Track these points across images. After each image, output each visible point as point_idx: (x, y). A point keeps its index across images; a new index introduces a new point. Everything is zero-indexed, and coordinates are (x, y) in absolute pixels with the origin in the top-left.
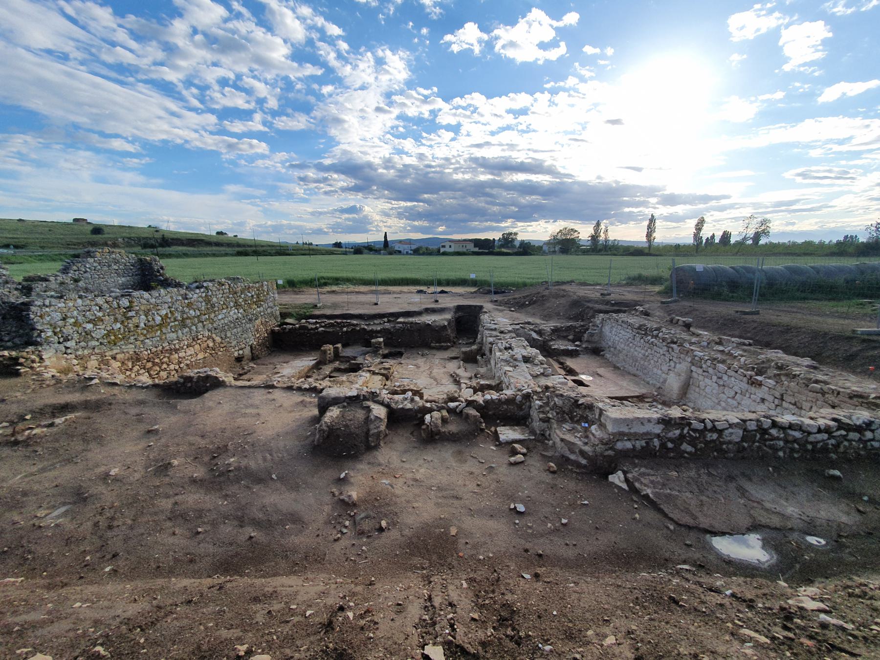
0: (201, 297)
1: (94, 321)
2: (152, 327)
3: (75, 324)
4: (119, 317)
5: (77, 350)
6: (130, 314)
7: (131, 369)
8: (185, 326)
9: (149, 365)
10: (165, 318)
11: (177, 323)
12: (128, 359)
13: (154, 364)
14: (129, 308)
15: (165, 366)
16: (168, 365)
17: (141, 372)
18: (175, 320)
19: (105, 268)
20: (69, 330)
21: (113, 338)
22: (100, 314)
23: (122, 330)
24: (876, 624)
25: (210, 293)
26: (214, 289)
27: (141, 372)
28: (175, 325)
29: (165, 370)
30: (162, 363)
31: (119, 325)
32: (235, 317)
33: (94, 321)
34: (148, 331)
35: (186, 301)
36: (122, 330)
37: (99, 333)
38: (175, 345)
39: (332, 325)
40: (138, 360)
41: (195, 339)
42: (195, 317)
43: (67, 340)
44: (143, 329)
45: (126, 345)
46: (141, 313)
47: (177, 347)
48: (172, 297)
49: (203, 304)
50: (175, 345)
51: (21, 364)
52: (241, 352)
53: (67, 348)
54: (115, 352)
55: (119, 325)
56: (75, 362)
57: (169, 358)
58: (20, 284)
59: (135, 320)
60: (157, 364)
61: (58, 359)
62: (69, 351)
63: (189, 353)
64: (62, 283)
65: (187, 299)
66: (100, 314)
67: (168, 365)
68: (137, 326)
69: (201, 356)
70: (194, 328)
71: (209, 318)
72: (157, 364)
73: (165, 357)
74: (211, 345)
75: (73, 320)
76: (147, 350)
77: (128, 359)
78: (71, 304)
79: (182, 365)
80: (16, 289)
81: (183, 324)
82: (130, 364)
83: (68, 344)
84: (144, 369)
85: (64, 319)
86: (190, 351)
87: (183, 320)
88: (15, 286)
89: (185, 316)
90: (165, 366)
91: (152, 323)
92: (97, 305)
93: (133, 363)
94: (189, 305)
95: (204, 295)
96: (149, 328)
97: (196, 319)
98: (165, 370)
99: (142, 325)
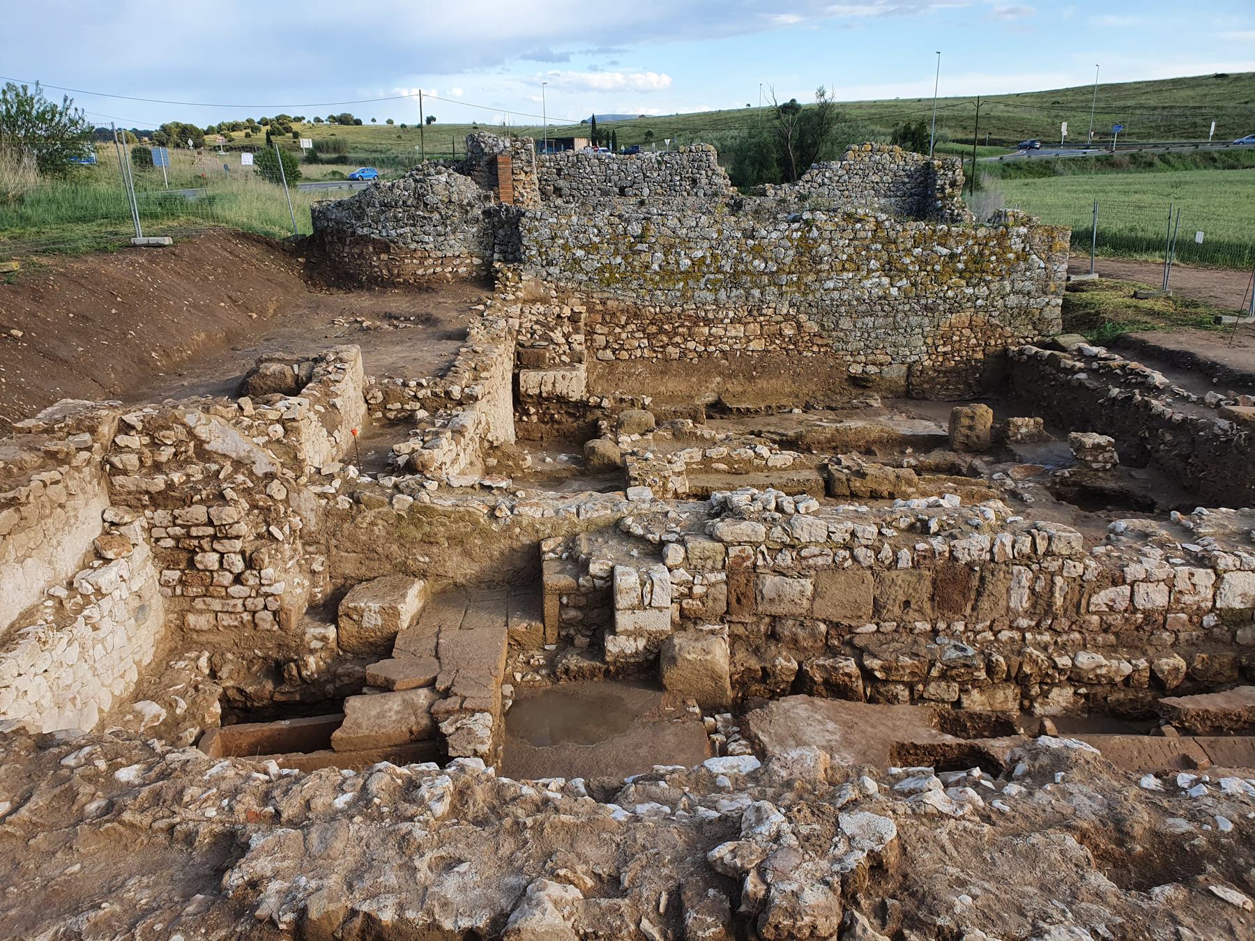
0: (791, 240)
1: (590, 248)
2: (672, 272)
3: (565, 247)
4: (622, 248)
5: (559, 280)
6: (639, 247)
7: (623, 327)
8: (737, 286)
9: (653, 329)
10: (698, 263)
11: (721, 276)
12: (622, 311)
13: (661, 331)
14: (641, 238)
15: (678, 339)
16: (686, 340)
17: (636, 335)
18: (719, 270)
19: (857, 180)
20: (555, 253)
21: (607, 275)
22: (597, 240)
23: (623, 268)
24: (4, 244)
25: (815, 233)
26: (830, 226)
27: (636, 335)
28: (717, 280)
29: (677, 345)
30: (676, 334)
31: (619, 260)
32: (877, 292)
33: (590, 248)
34: (662, 278)
35: (751, 242)
36: (623, 268)
37: (593, 263)
38: (706, 311)
39: (1107, 374)
40: (636, 316)
41: (755, 311)
42: (763, 273)
43: (550, 264)
44: (656, 273)
45: (624, 290)
46: (657, 247)
47: (710, 316)
48: (720, 232)
49: (791, 252)
50: (706, 311)
51: (498, 279)
52: (872, 369)
53: (549, 274)
54: (606, 295)
55: (619, 260)
56: (554, 293)
57: (689, 328)
58: (732, 197)
59: (645, 258)
60: (666, 333)
61: (536, 283)
62: (549, 279)
63: (733, 333)
64: (783, 201)
65: (753, 238)
66: (597, 240)
67: (686, 340)
68: (647, 267)
69: (757, 345)
70: (756, 293)
71: (798, 284)
72: (666, 333)
73: (682, 326)
74: (789, 331)
75: (562, 241)
76: (654, 307)
77: (622, 311)
78: (564, 221)
79: (712, 348)
80: (727, 205)
81: (734, 280)
82: (623, 319)
83: (551, 269)
84: (644, 331)
85: (553, 238)
86: (739, 331)
87: (735, 274)
88: (727, 200)
89: (741, 267)
90: (678, 339)
91: (673, 267)
92: (595, 226)
93: (628, 318)
94: (757, 252)
95: (797, 235)
96: (667, 274)
97: (766, 279)
98: (677, 345)
99: (656, 267)
